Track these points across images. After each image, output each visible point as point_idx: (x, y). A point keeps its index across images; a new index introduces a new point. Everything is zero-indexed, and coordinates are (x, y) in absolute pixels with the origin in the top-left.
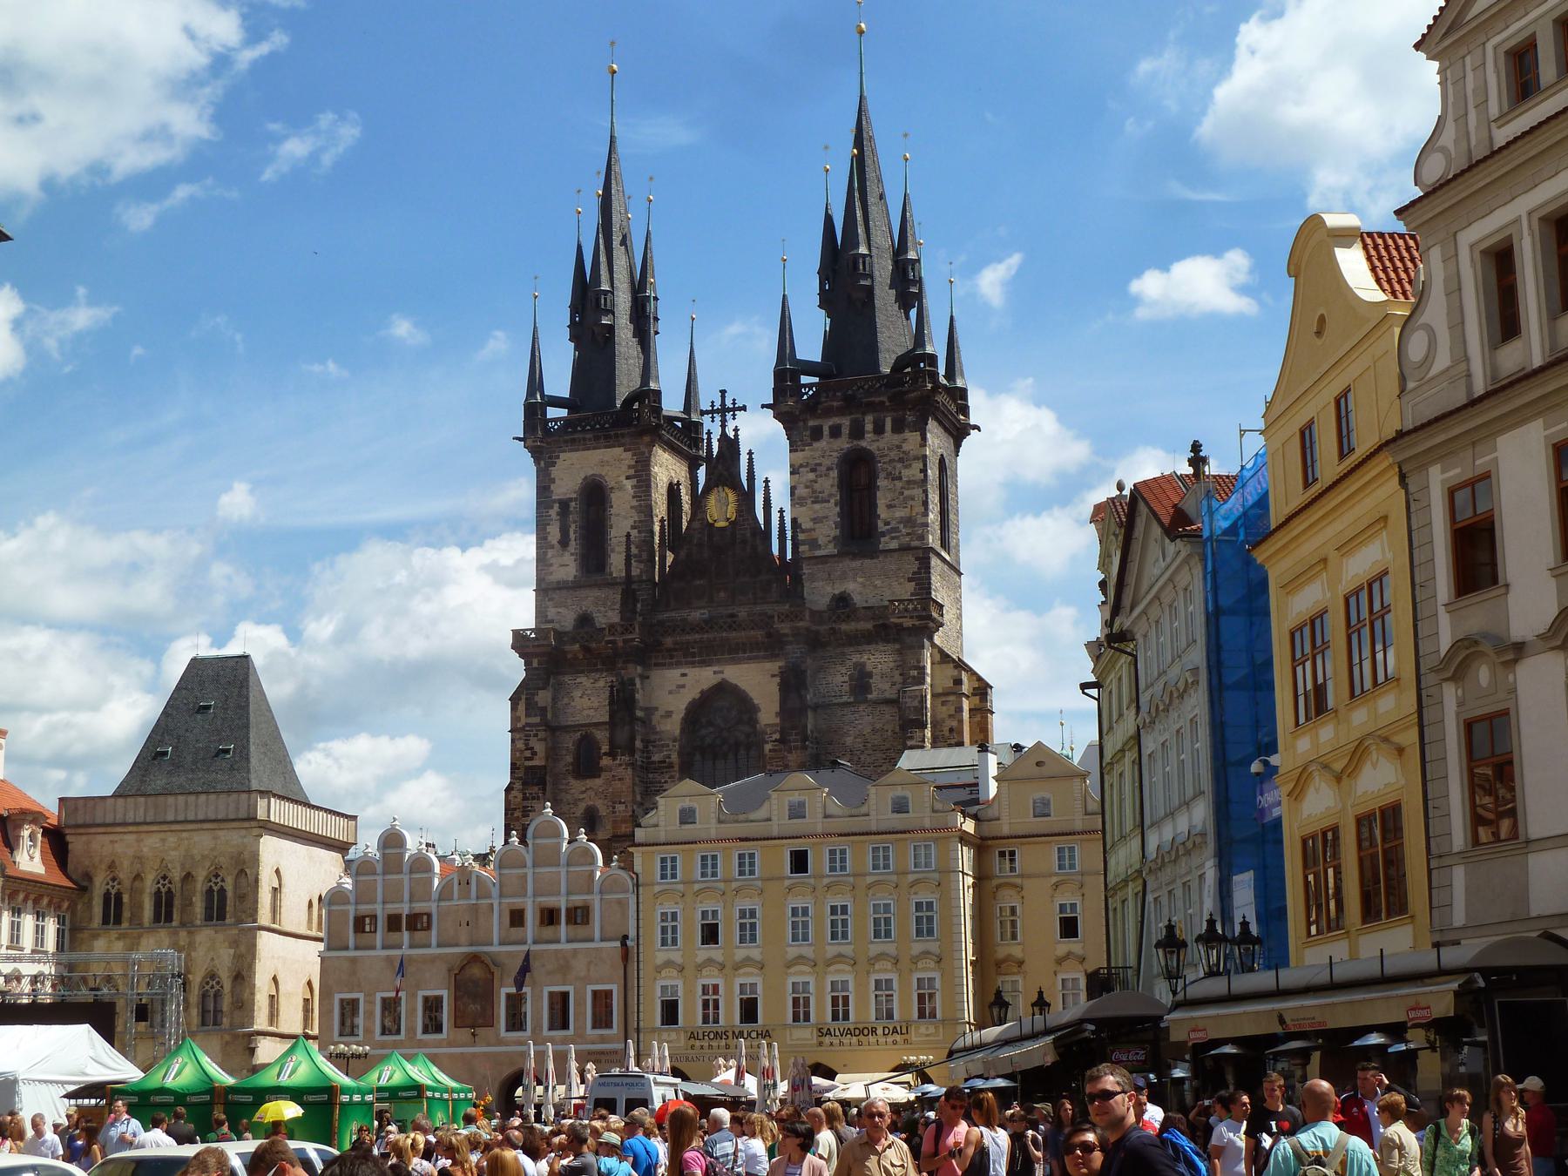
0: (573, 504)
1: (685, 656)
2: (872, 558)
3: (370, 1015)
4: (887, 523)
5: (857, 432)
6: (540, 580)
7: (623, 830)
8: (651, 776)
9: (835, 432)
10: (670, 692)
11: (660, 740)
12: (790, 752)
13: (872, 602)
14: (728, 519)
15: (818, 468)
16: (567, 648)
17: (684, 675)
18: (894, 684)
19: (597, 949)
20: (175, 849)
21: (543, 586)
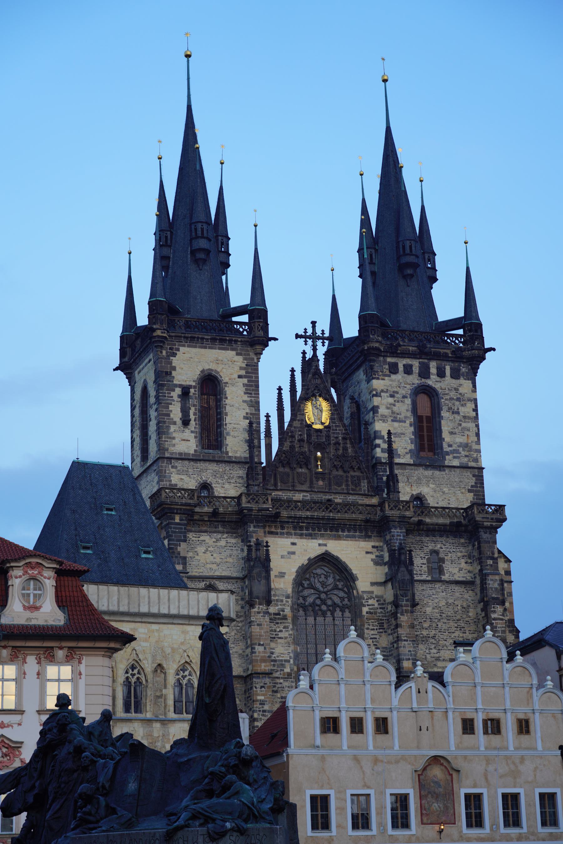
0: (192, 391)
1: (295, 528)
2: (440, 470)
3: (341, 810)
4: (450, 446)
5: (424, 373)
6: (161, 449)
7: (263, 667)
9: (408, 370)
10: (282, 557)
12: (402, 614)
13: (440, 504)
14: (322, 424)
15: (397, 395)
16: (197, 509)
17: (293, 544)
18: (461, 570)
19: (541, 757)
20: (146, 640)
21: (167, 455)
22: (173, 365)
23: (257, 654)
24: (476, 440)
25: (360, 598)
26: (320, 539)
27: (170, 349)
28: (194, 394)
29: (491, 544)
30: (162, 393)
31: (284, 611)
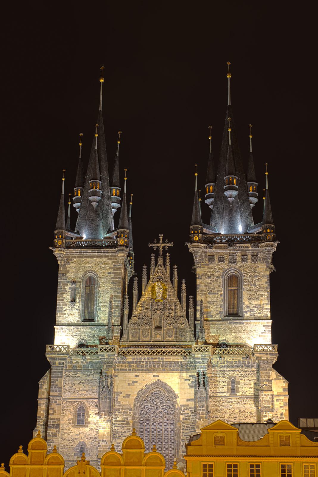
1: (138, 366)
4: (248, 307)
8: (116, 428)
9: (221, 260)
10: (129, 385)
11: (122, 409)
12: (199, 419)
17: (136, 376)
18: (250, 388)
22: (68, 269)
23: (101, 447)
24: (267, 302)
25: (180, 409)
26: (154, 372)
27: (67, 260)
28: (79, 286)
29: (268, 371)
30: (59, 287)
31: (127, 419)
